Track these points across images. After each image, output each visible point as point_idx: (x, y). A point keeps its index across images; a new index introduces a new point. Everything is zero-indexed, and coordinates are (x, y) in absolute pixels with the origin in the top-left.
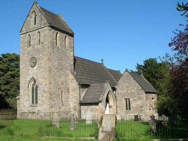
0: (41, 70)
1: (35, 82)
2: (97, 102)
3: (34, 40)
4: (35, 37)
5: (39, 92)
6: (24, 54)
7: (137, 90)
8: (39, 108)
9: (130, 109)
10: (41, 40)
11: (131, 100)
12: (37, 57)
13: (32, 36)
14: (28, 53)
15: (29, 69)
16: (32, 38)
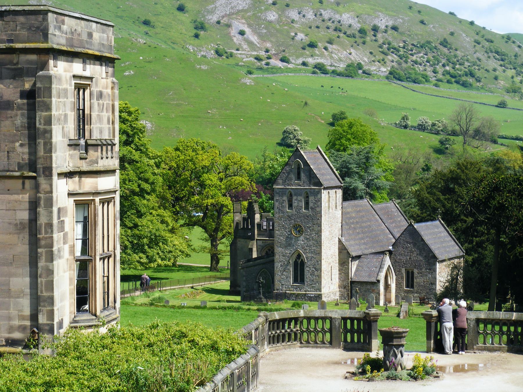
2: (375, 281)
5: (306, 269)
7: (425, 256)
9: (412, 287)
10: (311, 205)
11: (416, 271)
15: (291, 239)
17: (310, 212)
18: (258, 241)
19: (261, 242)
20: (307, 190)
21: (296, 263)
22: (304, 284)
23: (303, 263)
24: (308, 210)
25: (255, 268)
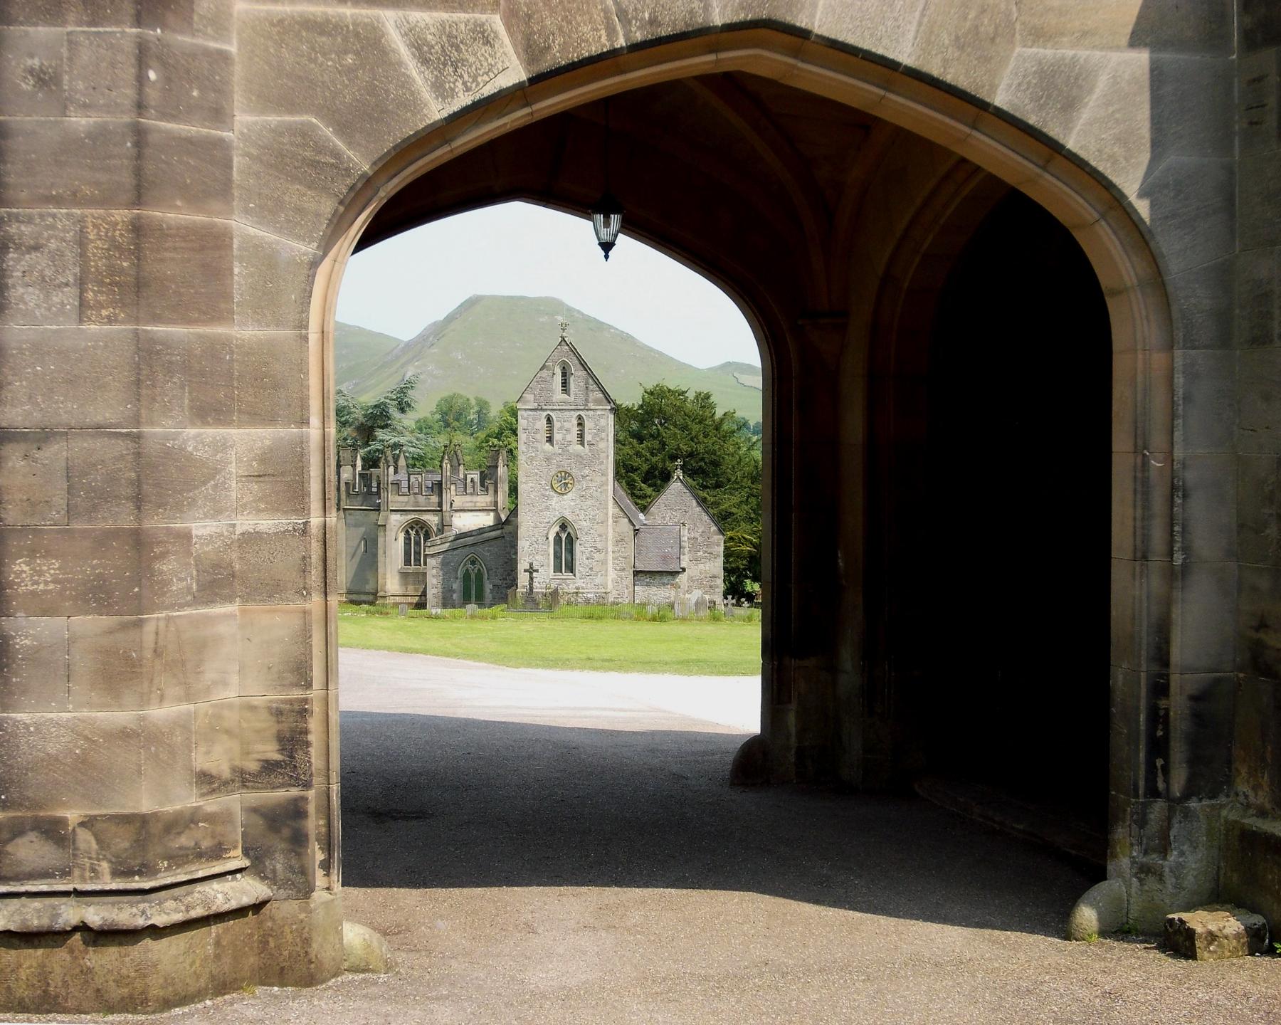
0: (588, 502)
1: (563, 527)
4: (567, 425)
5: (578, 549)
6: (532, 459)
8: (579, 583)
10: (588, 437)
12: (574, 472)
14: (548, 459)
15: (549, 497)
16: (557, 425)
21: (558, 540)
23: (571, 541)
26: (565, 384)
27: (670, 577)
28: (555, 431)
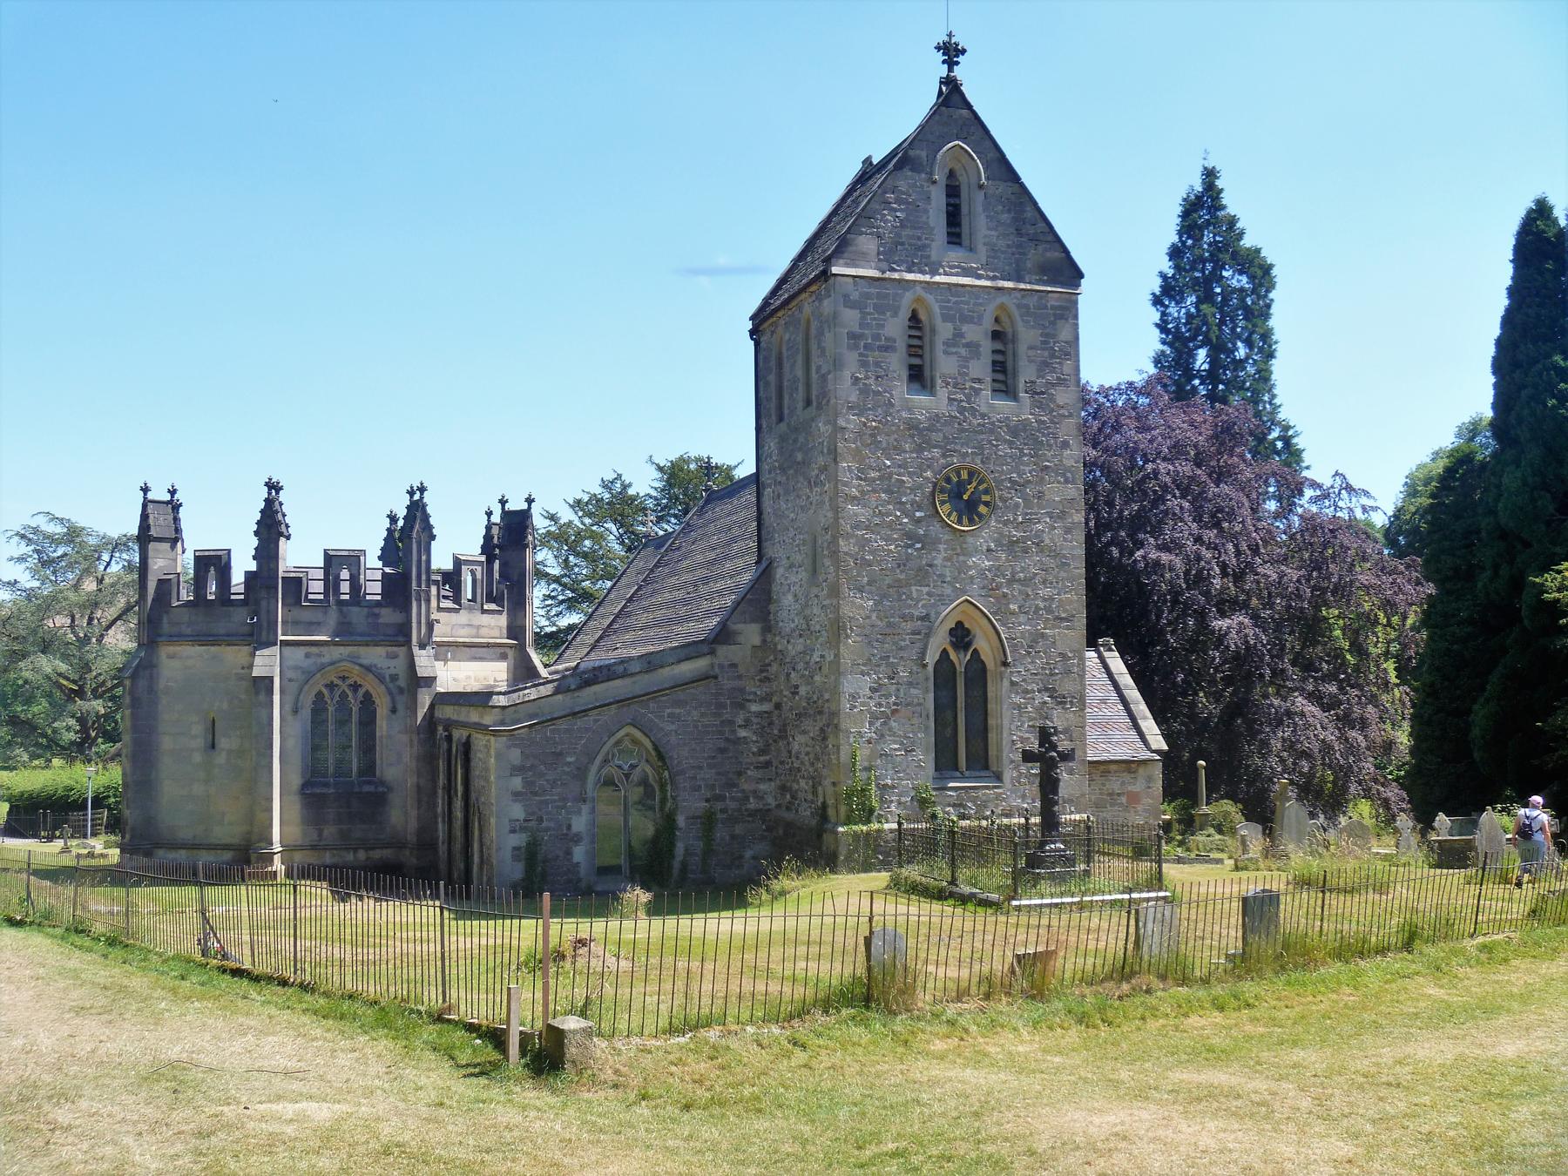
3: (963, 351)
10: (1026, 374)
13: (946, 318)
15: (928, 543)
17: (1018, 410)
18: (287, 650)
19: (302, 651)
20: (1004, 299)
22: (998, 777)
23: (978, 673)
24: (1015, 398)
25: (580, 723)
26: (954, 217)
27: (1127, 777)
28: (940, 347)
